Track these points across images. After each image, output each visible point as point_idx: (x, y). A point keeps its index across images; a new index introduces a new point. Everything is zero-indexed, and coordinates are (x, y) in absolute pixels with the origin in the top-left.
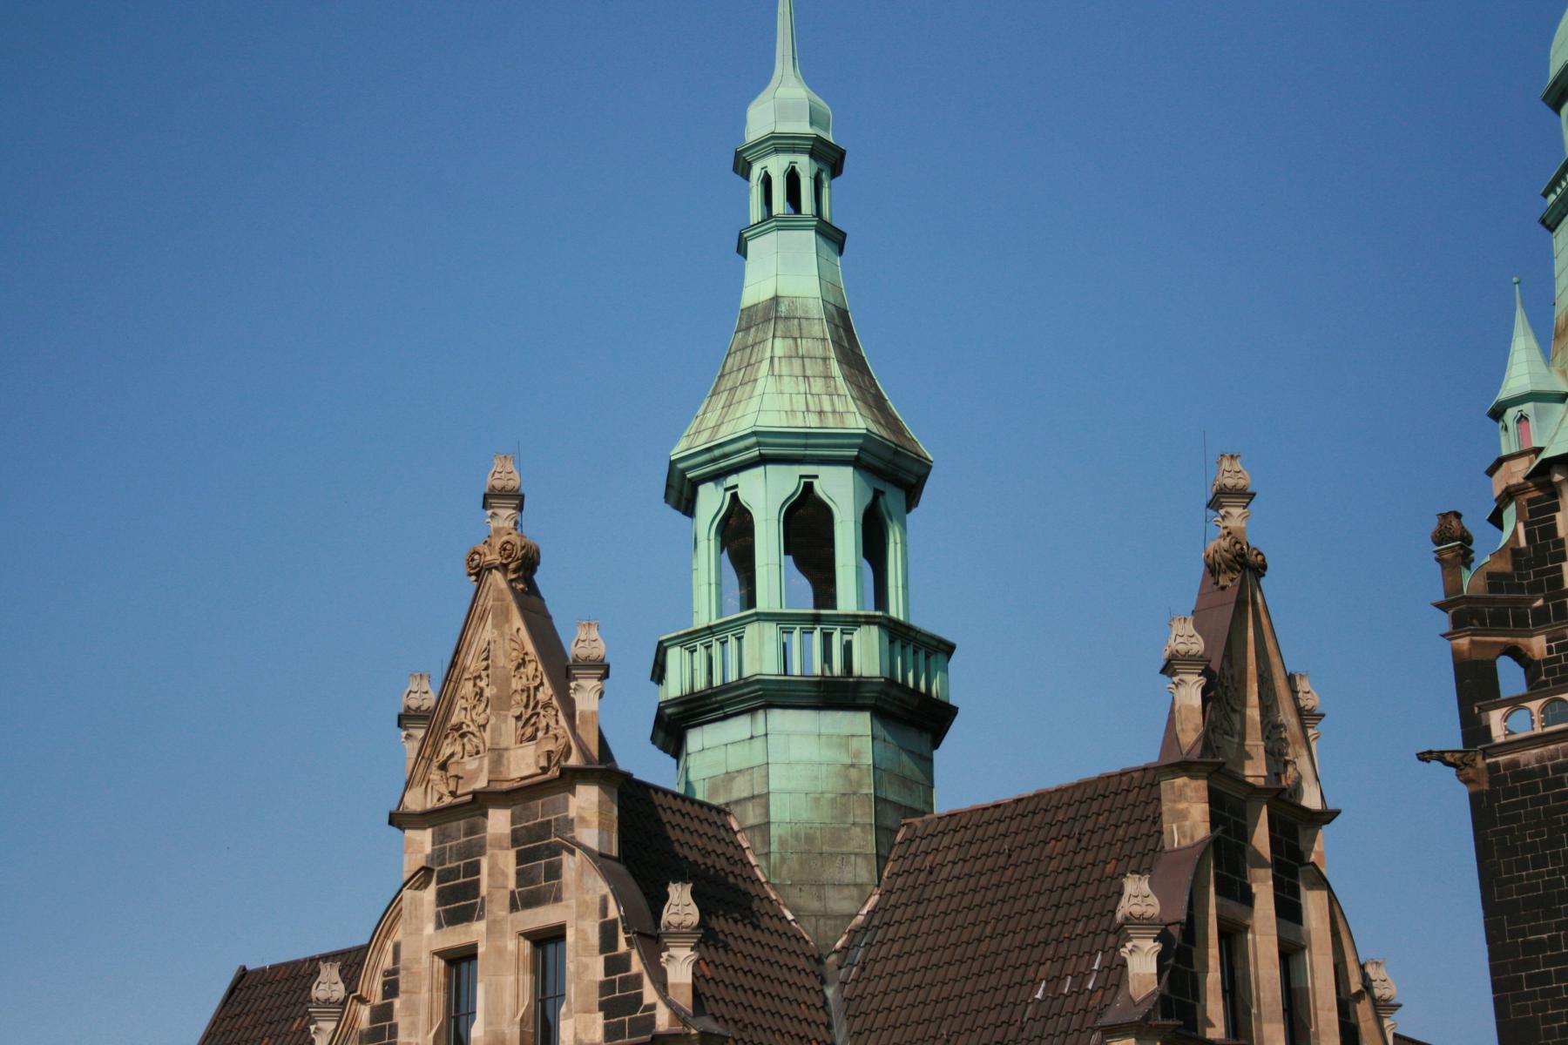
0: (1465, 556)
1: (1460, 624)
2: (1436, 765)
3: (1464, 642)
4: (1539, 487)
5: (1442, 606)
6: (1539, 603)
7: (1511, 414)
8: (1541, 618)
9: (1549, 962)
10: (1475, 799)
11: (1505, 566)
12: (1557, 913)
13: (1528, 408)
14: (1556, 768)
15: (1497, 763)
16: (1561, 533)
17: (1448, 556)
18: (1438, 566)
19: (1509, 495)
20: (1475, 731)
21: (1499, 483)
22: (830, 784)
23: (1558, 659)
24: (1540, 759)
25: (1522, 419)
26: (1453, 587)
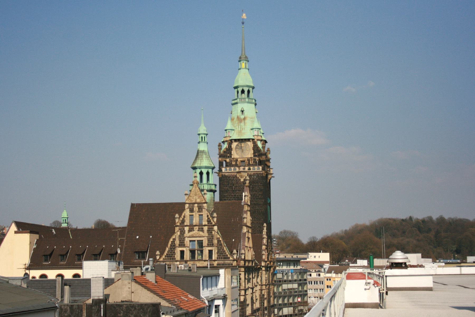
1: (220, 157)
2: (216, 173)
3: (220, 159)
4: (230, 141)
5: (218, 154)
6: (228, 155)
7: (228, 131)
8: (229, 157)
9: (226, 198)
10: (220, 178)
12: (228, 193)
13: (230, 131)
14: (230, 176)
15: (223, 174)
16: (232, 147)
17: (219, 148)
18: (218, 149)
19: (226, 141)
21: (225, 139)
23: (230, 162)
24: (228, 175)
25: (229, 132)
26: (220, 153)
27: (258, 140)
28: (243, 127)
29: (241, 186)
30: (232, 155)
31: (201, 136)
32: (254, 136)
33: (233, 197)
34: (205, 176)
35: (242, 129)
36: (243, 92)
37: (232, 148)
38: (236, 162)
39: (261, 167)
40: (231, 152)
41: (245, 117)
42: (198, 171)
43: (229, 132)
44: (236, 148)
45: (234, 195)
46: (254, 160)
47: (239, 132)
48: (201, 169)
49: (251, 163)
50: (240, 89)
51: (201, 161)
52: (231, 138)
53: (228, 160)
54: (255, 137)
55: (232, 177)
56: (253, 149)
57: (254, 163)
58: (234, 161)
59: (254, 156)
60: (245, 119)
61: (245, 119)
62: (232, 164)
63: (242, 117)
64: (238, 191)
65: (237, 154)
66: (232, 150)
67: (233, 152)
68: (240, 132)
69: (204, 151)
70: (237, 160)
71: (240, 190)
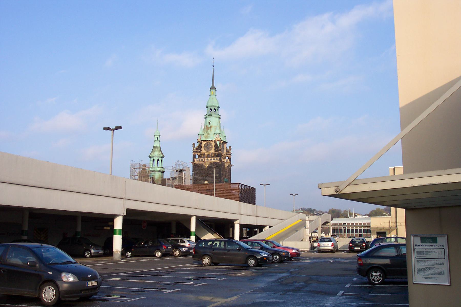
0: (194, 147)
1: (194, 152)
3: (194, 153)
10: (193, 166)
11: (197, 148)
13: (201, 135)
16: (202, 146)
20: (194, 161)
22: (159, 177)
27: (217, 141)
28: (209, 133)
29: (206, 171)
31: (155, 137)
33: (201, 178)
34: (155, 162)
39: (218, 158)
42: (152, 159)
43: (200, 136)
45: (201, 177)
49: (213, 156)
50: (209, 108)
51: (154, 153)
53: (199, 154)
58: (203, 155)
59: (215, 151)
60: (211, 127)
61: (211, 127)
63: (209, 126)
64: (204, 174)
67: (203, 149)
68: (207, 136)
69: (156, 146)
70: (204, 154)
71: (205, 174)
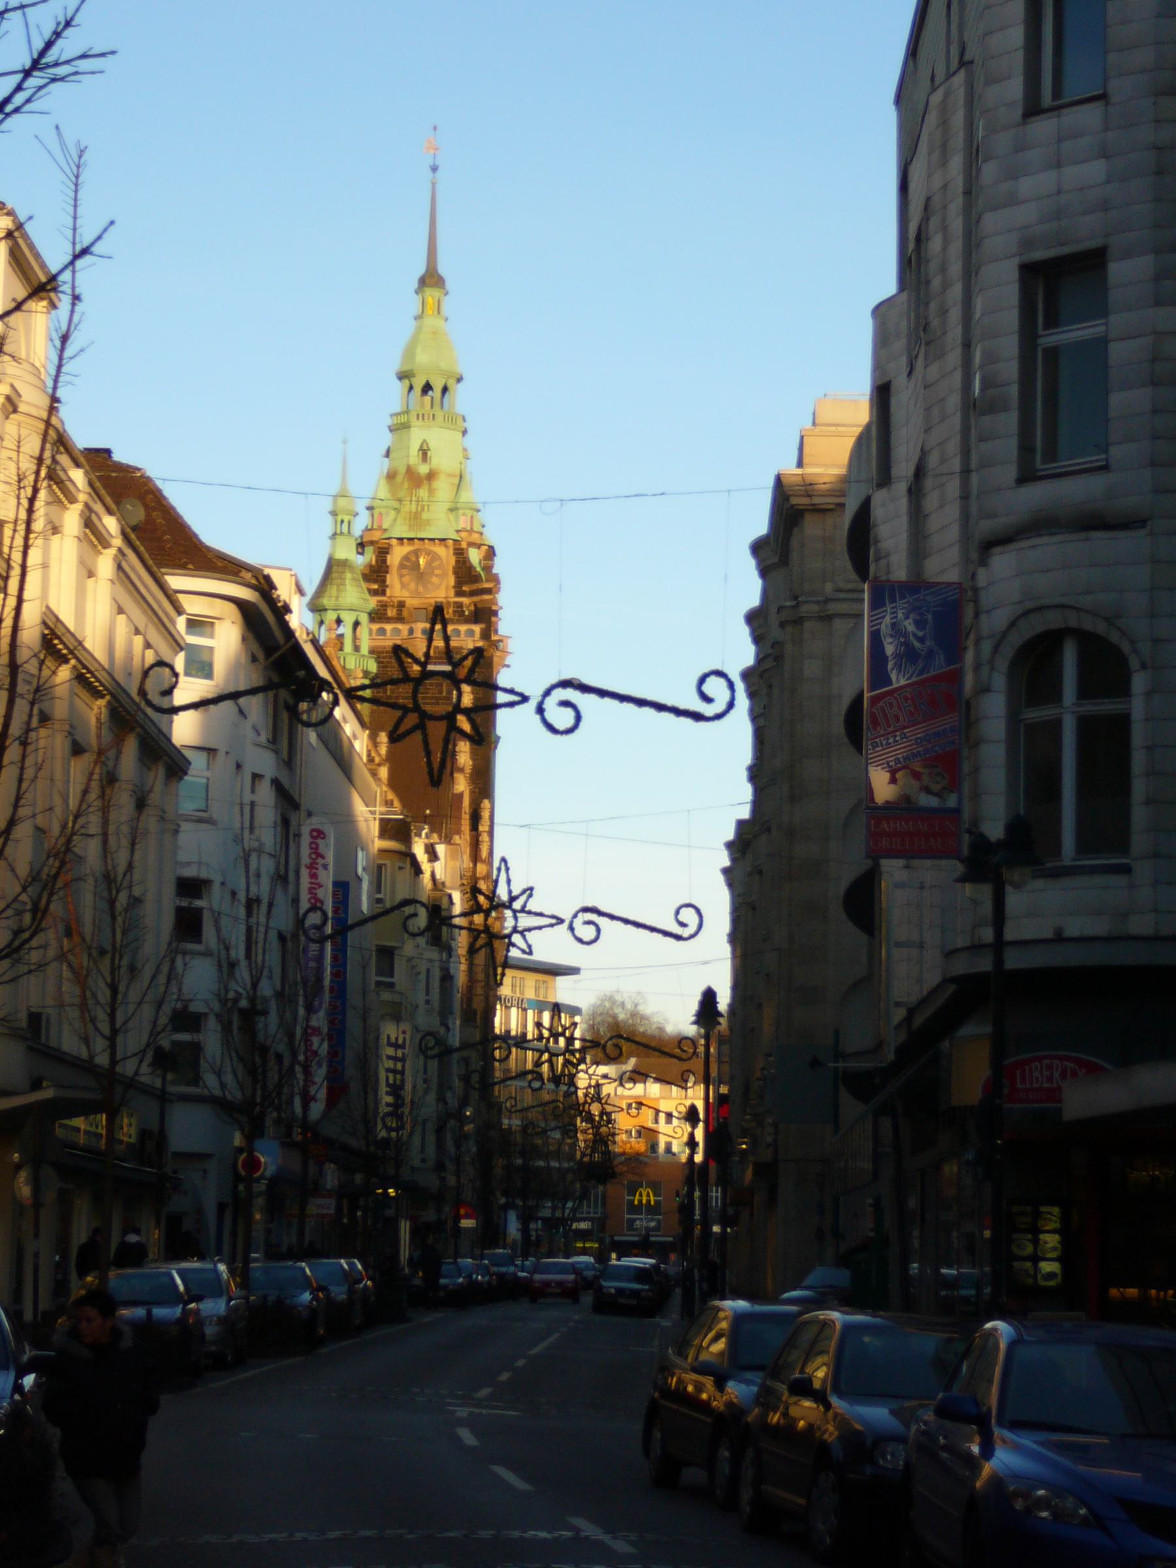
16: (388, 563)
19: (372, 543)
30: (387, 586)
32: (458, 531)
35: (423, 509)
36: (427, 388)
37: (387, 567)
38: (400, 611)
40: (385, 576)
41: (431, 470)
44: (402, 566)
46: (458, 607)
47: (412, 517)
48: (339, 612)
51: (338, 590)
52: (386, 535)
54: (463, 534)
55: (385, 655)
56: (456, 573)
57: (454, 615)
58: (393, 606)
60: (431, 476)
62: (386, 614)
63: (423, 469)
65: (403, 585)
66: (387, 572)
67: (392, 579)
70: (401, 605)
